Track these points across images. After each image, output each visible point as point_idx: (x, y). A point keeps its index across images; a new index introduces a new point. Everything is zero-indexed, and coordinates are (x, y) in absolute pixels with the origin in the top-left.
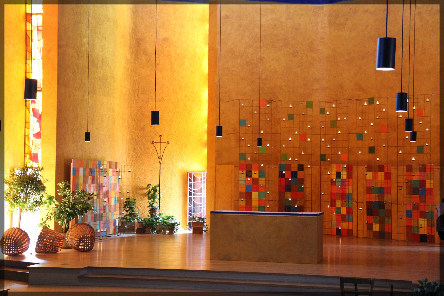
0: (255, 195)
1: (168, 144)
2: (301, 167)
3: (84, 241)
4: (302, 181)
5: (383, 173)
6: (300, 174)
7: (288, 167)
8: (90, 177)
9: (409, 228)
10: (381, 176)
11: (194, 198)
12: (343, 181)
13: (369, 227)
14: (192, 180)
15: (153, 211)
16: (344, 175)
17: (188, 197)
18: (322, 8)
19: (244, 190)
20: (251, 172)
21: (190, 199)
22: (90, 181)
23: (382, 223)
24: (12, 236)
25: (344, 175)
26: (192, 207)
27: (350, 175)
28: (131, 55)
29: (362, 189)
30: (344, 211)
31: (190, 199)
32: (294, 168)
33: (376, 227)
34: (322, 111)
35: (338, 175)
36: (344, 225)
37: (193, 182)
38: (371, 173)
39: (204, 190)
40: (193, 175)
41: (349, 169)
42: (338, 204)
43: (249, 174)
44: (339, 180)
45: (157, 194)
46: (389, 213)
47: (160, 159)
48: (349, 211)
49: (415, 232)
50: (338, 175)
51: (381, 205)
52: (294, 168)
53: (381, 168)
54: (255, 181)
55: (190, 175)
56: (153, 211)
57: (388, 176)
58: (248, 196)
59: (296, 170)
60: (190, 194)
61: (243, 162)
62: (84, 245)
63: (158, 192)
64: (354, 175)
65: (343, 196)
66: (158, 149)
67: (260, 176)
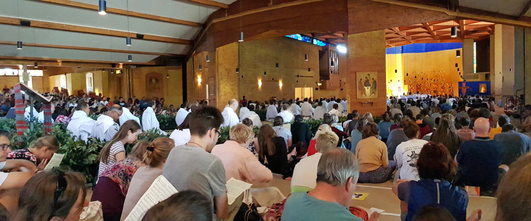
0: (412, 90)
2: (421, 85)
10: (436, 85)
15: (392, 94)
16: (429, 86)
25: (429, 86)
27: (430, 86)
29: (433, 88)
32: (420, 85)
34: (425, 74)
35: (428, 86)
41: (430, 84)
52: (420, 85)
53: (436, 84)
54: (412, 88)
56: (392, 94)
57: (437, 85)
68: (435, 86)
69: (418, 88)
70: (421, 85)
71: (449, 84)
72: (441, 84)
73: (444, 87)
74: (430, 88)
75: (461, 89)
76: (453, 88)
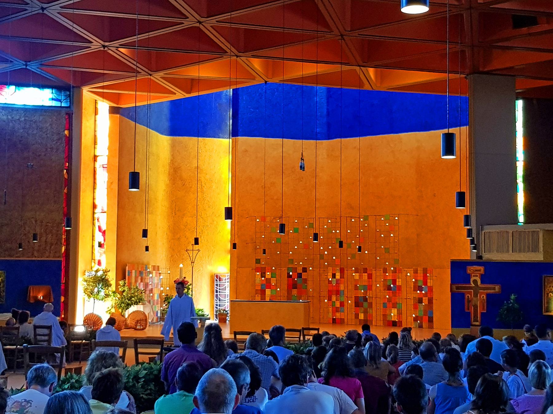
0: (268, 292)
1: (199, 251)
2: (305, 270)
3: (140, 322)
4: (305, 281)
5: (366, 274)
6: (304, 275)
7: (294, 270)
8: (140, 277)
9: (385, 316)
11: (220, 295)
12: (337, 281)
13: (357, 316)
14: (218, 280)
16: (338, 276)
17: (215, 293)
18: (322, 143)
19: (259, 288)
20: (265, 273)
21: (217, 295)
22: (139, 281)
23: (365, 312)
24: (90, 318)
25: (338, 276)
26: (218, 302)
27: (342, 276)
28: (169, 181)
29: (351, 287)
30: (338, 304)
31: (217, 295)
32: (300, 270)
33: (361, 316)
35: (334, 276)
36: (338, 315)
37: (219, 282)
38: (358, 274)
39: (228, 287)
40: (219, 277)
41: (342, 271)
42: (334, 298)
43: (263, 275)
44: (335, 279)
45: (190, 291)
46: (370, 305)
47: (193, 264)
48: (342, 304)
49: (389, 319)
50: (334, 276)
51: (365, 299)
52: (300, 270)
54: (268, 281)
55: (217, 276)
57: (370, 277)
58: (263, 292)
59: (301, 272)
60: (217, 292)
61: (258, 265)
62: (140, 326)
63: (191, 290)
64: (345, 276)
65: (338, 293)
66: (191, 255)
67: (272, 277)
68: (360, 276)
69: (293, 285)
70: (305, 270)
71: (416, 272)
72: (385, 271)
73: (394, 282)
74: (342, 287)
75: (463, 295)
76: (431, 289)
